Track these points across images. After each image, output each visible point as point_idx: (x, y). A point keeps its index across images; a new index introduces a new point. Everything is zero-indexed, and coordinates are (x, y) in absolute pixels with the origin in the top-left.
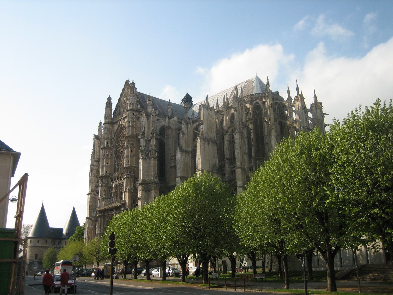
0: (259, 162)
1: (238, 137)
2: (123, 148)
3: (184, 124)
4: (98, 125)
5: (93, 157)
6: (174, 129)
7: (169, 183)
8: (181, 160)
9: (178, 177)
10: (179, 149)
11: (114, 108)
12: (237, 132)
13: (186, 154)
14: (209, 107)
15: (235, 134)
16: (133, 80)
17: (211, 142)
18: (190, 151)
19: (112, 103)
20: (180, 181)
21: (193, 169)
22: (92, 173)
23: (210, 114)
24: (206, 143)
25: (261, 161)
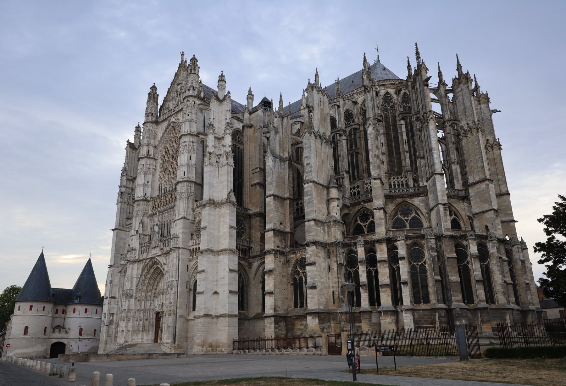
0: (394, 178)
1: (373, 132)
2: (174, 157)
3: (276, 117)
4: (135, 129)
5: (125, 174)
6: (258, 127)
7: (249, 209)
8: (273, 169)
9: (269, 196)
10: (271, 152)
11: (160, 102)
12: (371, 123)
13: (280, 161)
14: (320, 89)
15: (368, 127)
16: (194, 55)
17: (324, 141)
18: (287, 157)
19: (158, 95)
20: (272, 203)
21: (292, 185)
22: (121, 198)
23: (322, 99)
24: (319, 140)
25: (398, 178)
